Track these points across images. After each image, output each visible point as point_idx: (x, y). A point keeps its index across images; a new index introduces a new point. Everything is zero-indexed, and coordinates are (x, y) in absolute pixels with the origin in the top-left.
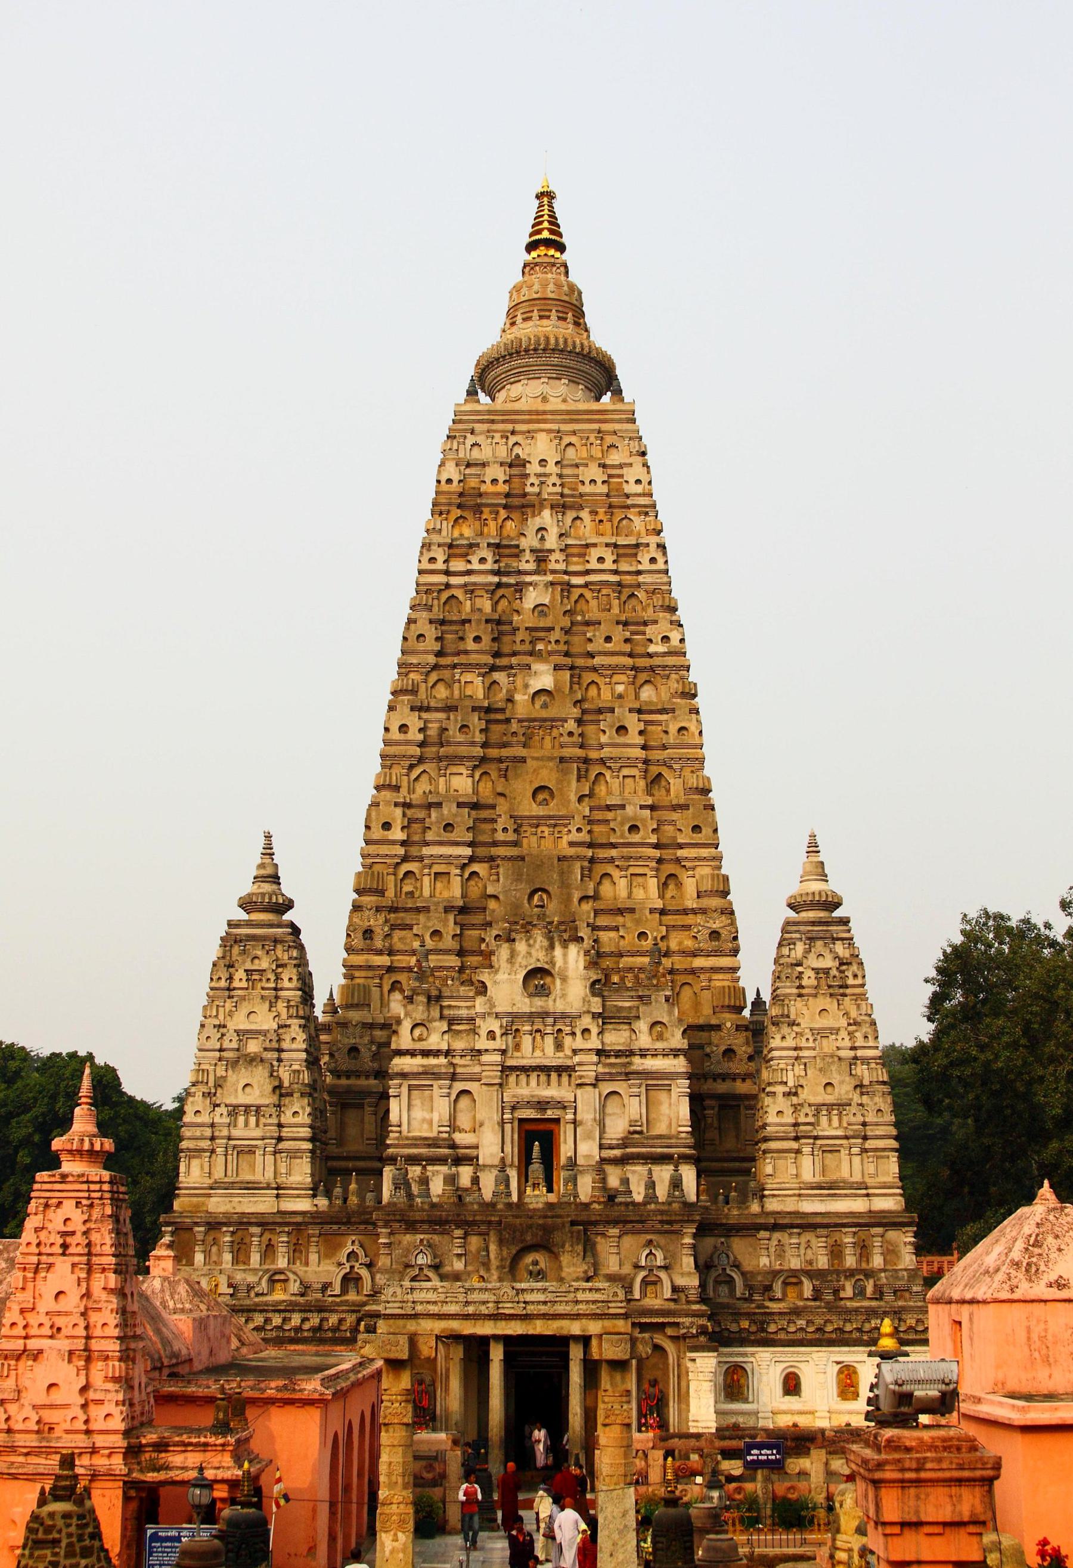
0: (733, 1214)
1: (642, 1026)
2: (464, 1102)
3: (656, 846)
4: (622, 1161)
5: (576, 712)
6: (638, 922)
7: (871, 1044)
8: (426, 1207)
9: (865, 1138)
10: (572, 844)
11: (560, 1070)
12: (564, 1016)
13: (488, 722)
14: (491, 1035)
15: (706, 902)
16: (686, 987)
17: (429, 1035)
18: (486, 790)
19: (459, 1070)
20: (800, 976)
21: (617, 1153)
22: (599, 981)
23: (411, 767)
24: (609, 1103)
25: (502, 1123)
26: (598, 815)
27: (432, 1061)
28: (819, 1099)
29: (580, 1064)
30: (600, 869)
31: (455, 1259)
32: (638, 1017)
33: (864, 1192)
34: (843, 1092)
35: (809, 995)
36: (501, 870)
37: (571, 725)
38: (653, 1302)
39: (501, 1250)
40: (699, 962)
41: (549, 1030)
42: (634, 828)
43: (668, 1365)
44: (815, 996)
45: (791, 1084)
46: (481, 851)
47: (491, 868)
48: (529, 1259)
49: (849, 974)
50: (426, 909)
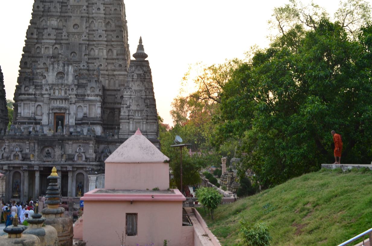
0: (110, 139)
1: (88, 88)
2: (39, 108)
3: (106, 41)
4: (80, 124)
5: (87, 4)
6: (100, 62)
7: (151, 94)
8: (19, 135)
9: (147, 119)
10: (83, 40)
12: (67, 85)
13: (62, 6)
14: (47, 90)
15: (119, 57)
16: (112, 79)
17: (29, 89)
18: (61, 24)
19: (37, 99)
20: (133, 76)
21: (80, 122)
22: (77, 76)
23: (40, 18)
24: (79, 109)
25: (49, 114)
26: (91, 32)
27: (30, 97)
28: (135, 109)
29: (71, 98)
30: (91, 47)
31: (26, 149)
32: (87, 86)
33: (146, 134)
34: (142, 107)
35: (135, 81)
36: (63, 47)
37: (85, 7)
38: (80, 162)
39: (38, 147)
40: (115, 73)
41: (63, 89)
42: (100, 36)
43: (84, 178)
44: (137, 81)
45: (128, 104)
46: (58, 42)
48: (46, 149)
49: (146, 75)
50: (42, 57)
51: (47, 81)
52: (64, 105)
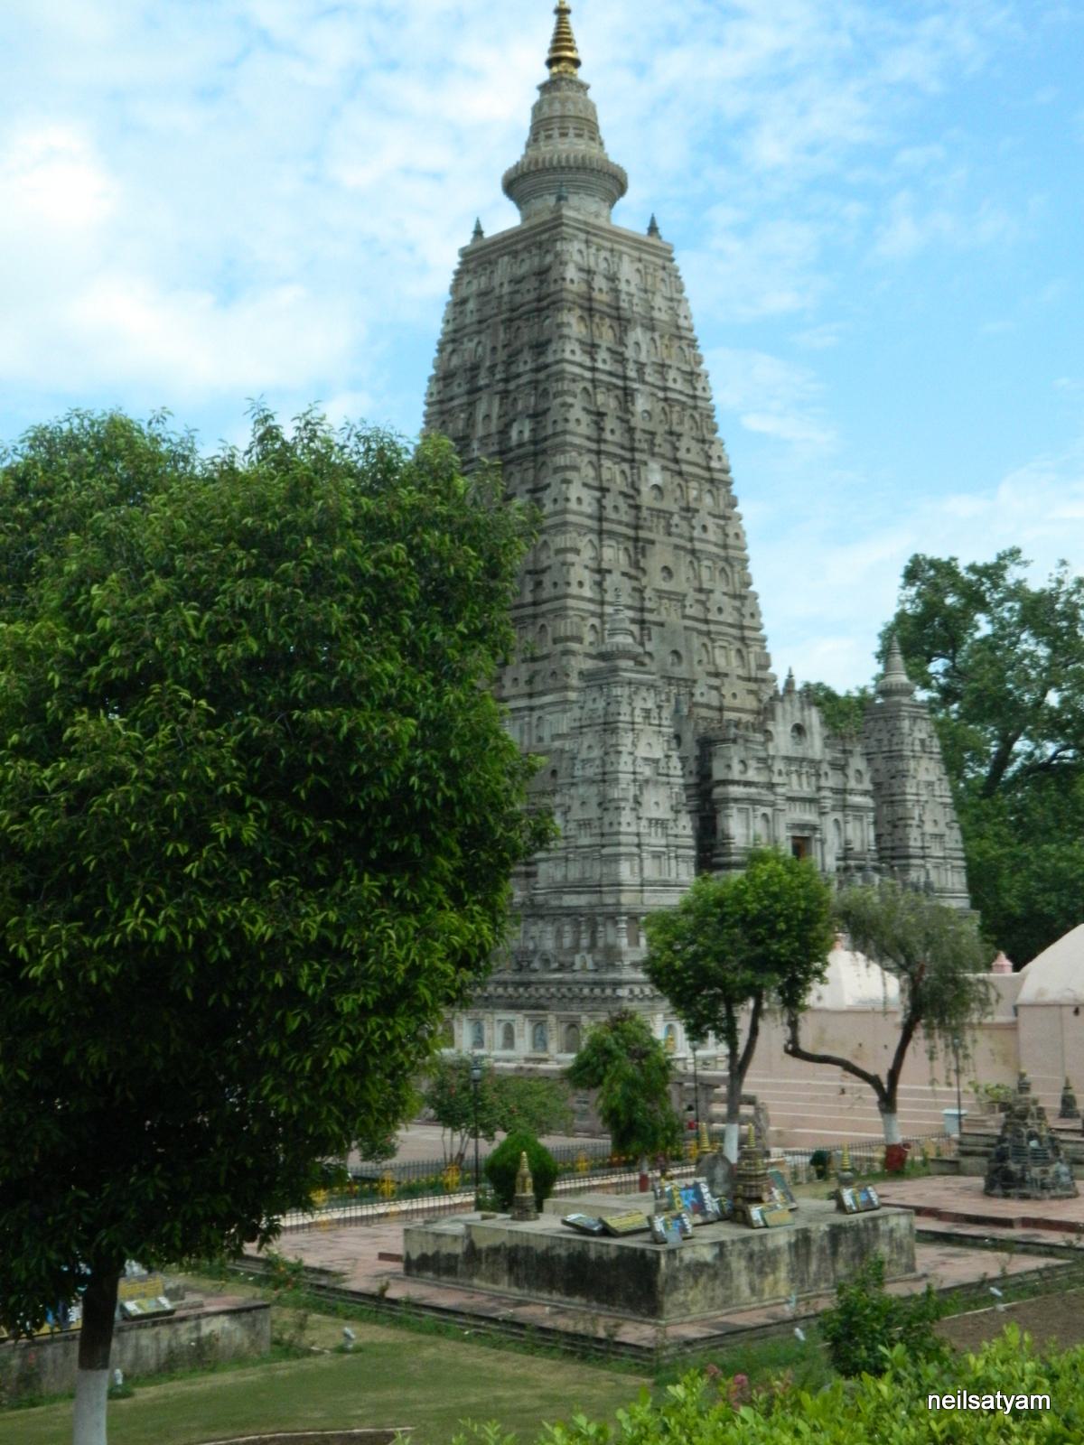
11: (811, 801)
27: (753, 790)
47: (642, 629)
51: (776, 748)
52: (809, 816)
